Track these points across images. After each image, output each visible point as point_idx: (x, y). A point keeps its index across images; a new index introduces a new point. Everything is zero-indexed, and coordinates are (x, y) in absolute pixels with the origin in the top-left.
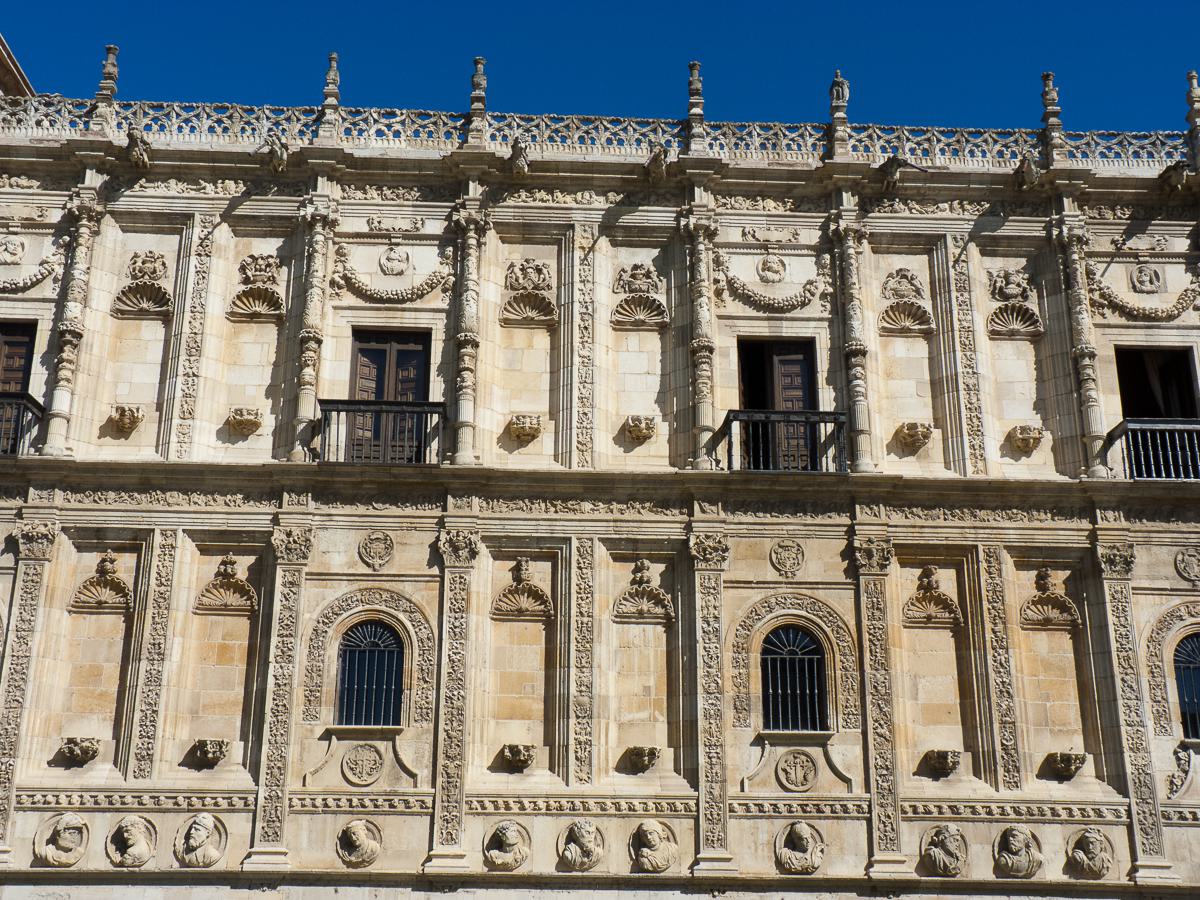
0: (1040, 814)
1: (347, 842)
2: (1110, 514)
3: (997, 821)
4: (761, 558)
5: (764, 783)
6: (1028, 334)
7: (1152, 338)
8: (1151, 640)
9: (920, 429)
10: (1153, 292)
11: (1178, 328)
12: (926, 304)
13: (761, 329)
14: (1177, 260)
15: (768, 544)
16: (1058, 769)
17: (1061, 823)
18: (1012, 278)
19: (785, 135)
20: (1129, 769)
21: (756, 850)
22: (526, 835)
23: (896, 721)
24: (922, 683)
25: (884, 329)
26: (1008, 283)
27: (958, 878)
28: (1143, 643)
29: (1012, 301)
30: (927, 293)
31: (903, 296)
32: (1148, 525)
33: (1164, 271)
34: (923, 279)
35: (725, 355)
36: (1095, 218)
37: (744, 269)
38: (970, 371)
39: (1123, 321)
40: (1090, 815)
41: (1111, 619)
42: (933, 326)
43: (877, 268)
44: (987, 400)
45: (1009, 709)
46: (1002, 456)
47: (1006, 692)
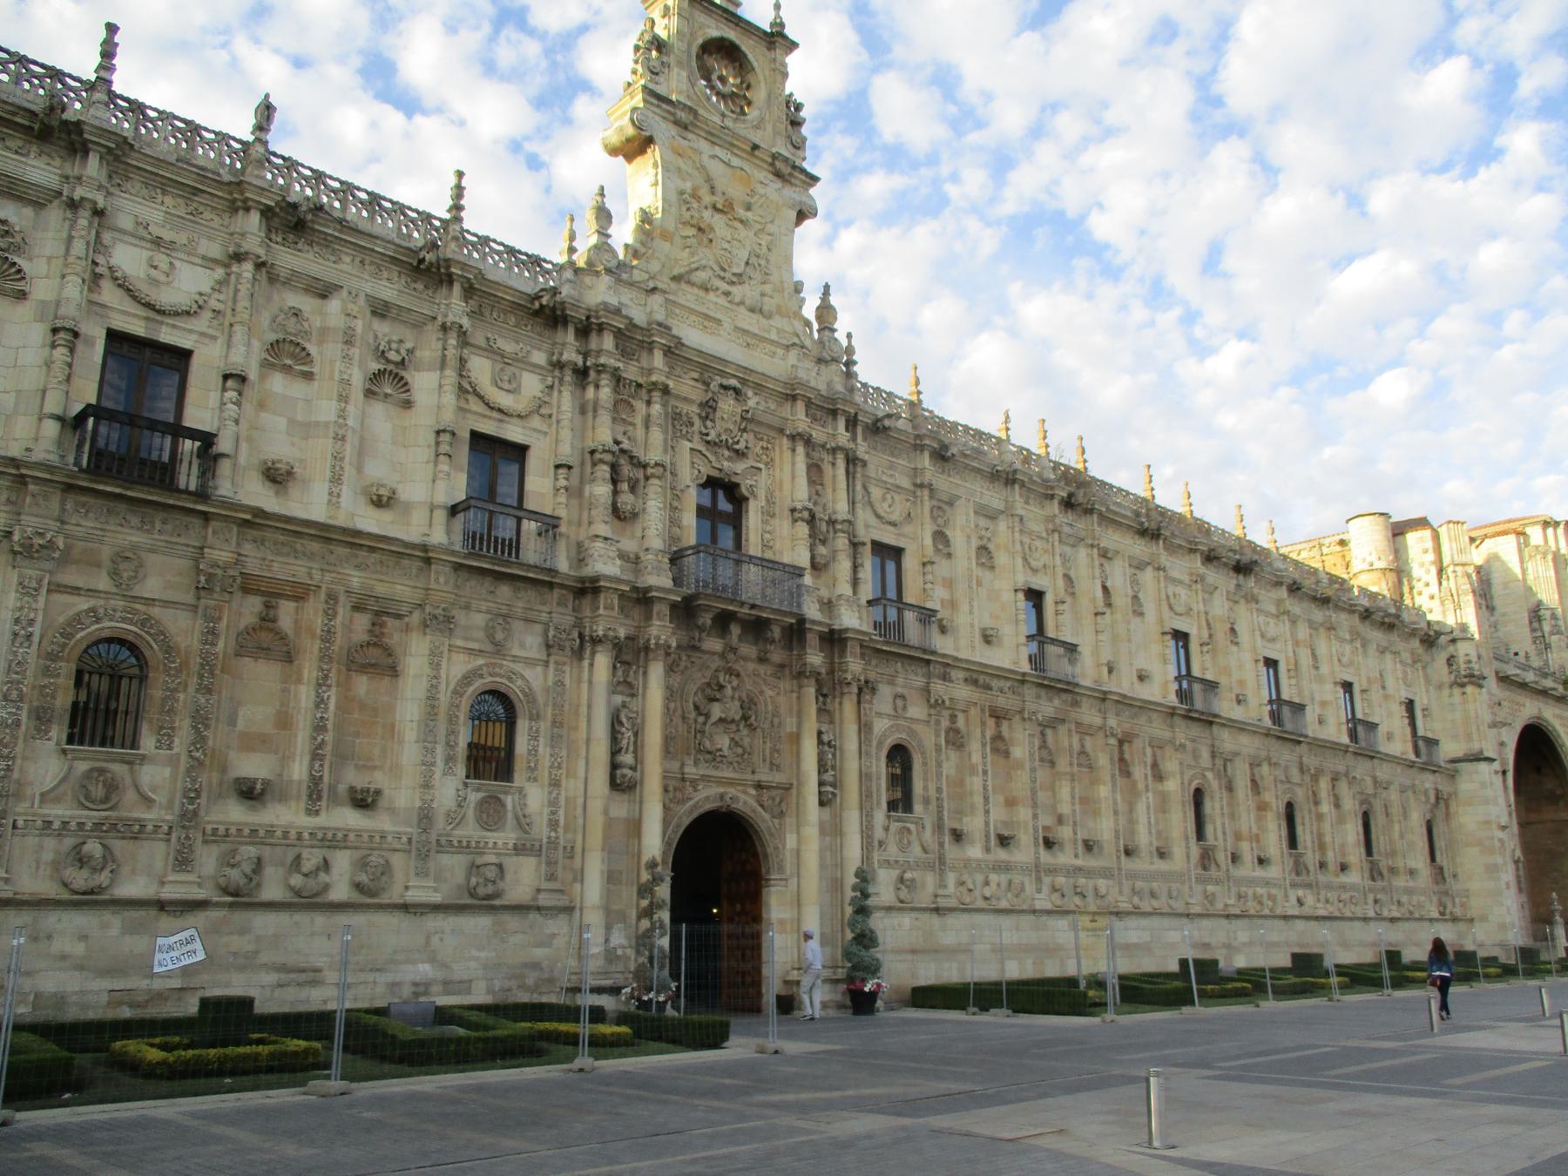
0: (332, 841)
4: (98, 565)
5: (57, 800)
8: (455, 692)
13: (137, 328)
15: (106, 552)
21: (38, 867)
35: (90, 343)
37: (128, 259)
38: (341, 421)
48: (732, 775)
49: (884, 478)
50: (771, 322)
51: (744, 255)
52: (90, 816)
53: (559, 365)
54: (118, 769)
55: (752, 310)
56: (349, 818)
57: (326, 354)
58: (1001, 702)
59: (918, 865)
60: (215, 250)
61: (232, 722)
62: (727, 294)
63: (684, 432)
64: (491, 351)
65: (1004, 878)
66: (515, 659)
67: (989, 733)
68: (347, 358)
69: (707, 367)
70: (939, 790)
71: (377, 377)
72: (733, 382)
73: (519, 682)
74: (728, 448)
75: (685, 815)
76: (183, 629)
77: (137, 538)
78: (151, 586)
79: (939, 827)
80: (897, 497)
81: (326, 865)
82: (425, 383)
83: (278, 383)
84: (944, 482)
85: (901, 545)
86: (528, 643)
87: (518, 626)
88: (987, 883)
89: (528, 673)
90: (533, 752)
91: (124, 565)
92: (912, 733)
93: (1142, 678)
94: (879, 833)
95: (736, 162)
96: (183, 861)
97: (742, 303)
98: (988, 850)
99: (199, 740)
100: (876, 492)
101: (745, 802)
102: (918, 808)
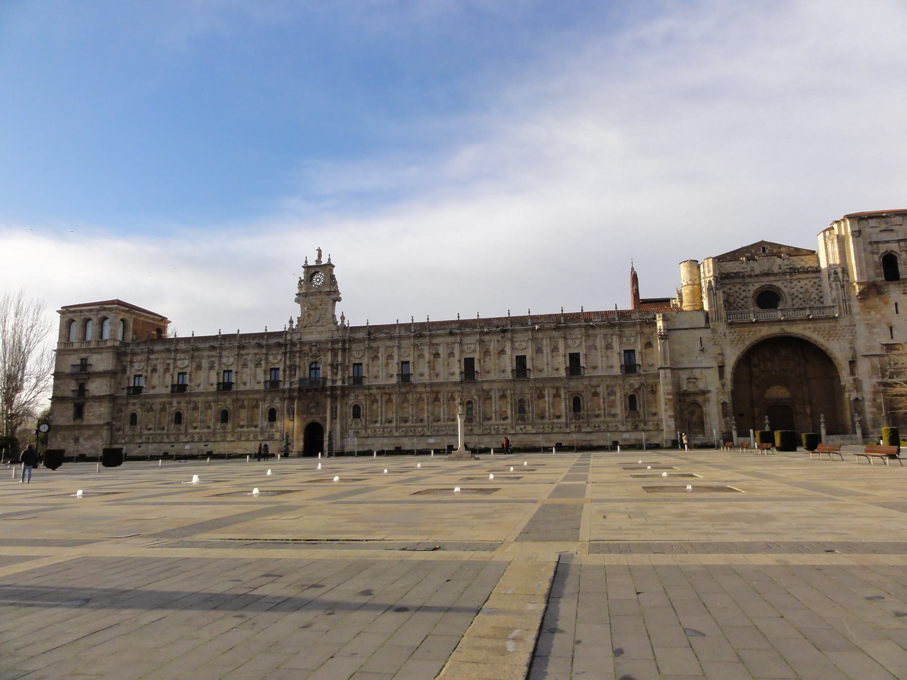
0: (250, 432)
1: (175, 438)
13: (226, 369)
22: (193, 437)
40: (254, 432)
51: (319, 316)
52: (223, 431)
53: (283, 353)
54: (225, 425)
55: (321, 326)
56: (253, 429)
57: (249, 363)
58: (387, 391)
59: (361, 428)
60: (233, 355)
61: (239, 417)
64: (273, 354)
65: (386, 430)
67: (384, 399)
68: (251, 363)
69: (310, 343)
70: (366, 413)
71: (257, 364)
72: (314, 344)
75: (305, 424)
76: (231, 407)
77: (225, 397)
78: (228, 403)
79: (366, 420)
80: (360, 352)
81: (249, 435)
82: (263, 362)
83: (245, 370)
84: (374, 345)
86: (277, 400)
88: (380, 431)
89: (276, 405)
90: (278, 417)
91: (225, 401)
92: (360, 402)
93: (453, 374)
96: (232, 436)
97: (319, 326)
98: (381, 424)
99: (233, 421)
101: (318, 420)
102: (361, 417)
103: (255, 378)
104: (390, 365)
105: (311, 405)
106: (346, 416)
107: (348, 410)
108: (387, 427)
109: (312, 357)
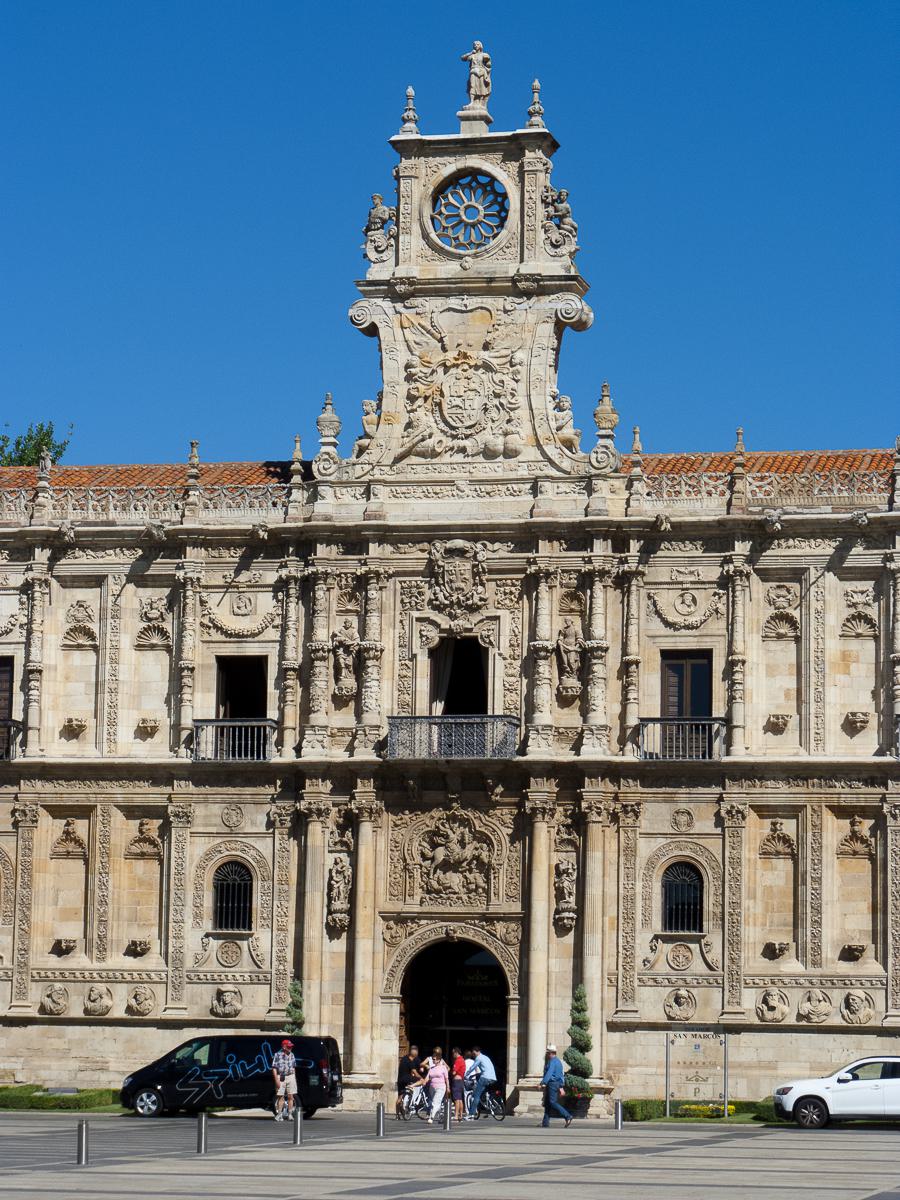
0: (112, 978)
2: (183, 783)
3: (88, 982)
6: (163, 646)
7: (240, 650)
8: (199, 867)
9: (75, 722)
10: (246, 615)
11: (259, 642)
12: (95, 627)
14: (267, 589)
16: (135, 950)
17: (127, 982)
18: (155, 605)
19: (7, 498)
20: (171, 949)
23: (32, 920)
24: (61, 894)
25: (65, 645)
26: (152, 609)
27: (62, 1016)
28: (193, 869)
29: (154, 623)
30: (96, 618)
31: (79, 621)
32: (207, 789)
33: (256, 598)
34: (95, 609)
36: (215, 557)
39: (223, 638)
40: (144, 979)
41: (174, 853)
42: (97, 643)
43: (64, 599)
44: (122, 699)
45: (105, 911)
46: (135, 738)
47: (104, 902)
48: (459, 910)
49: (681, 578)
50: (520, 458)
51: (478, 403)
62: (463, 450)
63: (413, 604)
66: (247, 835)
70: (736, 904)
72: (459, 543)
73: (252, 852)
74: (460, 607)
85: (704, 644)
87: (248, 809)
94: (642, 950)
95: (473, 302)
100: (667, 599)
103: (136, 700)
104: (853, 666)
105: (440, 853)
106: (630, 917)
107: (639, 885)
108: (845, 981)
109: (439, 608)
